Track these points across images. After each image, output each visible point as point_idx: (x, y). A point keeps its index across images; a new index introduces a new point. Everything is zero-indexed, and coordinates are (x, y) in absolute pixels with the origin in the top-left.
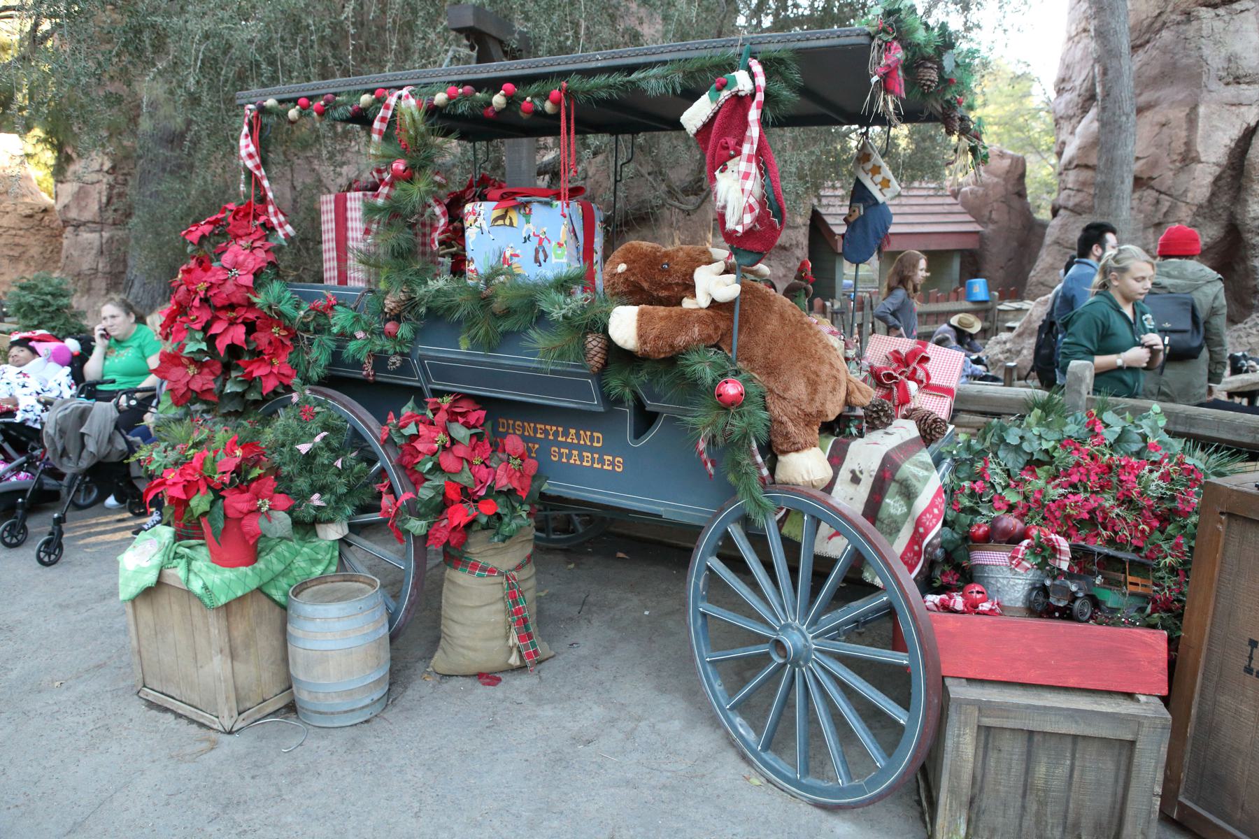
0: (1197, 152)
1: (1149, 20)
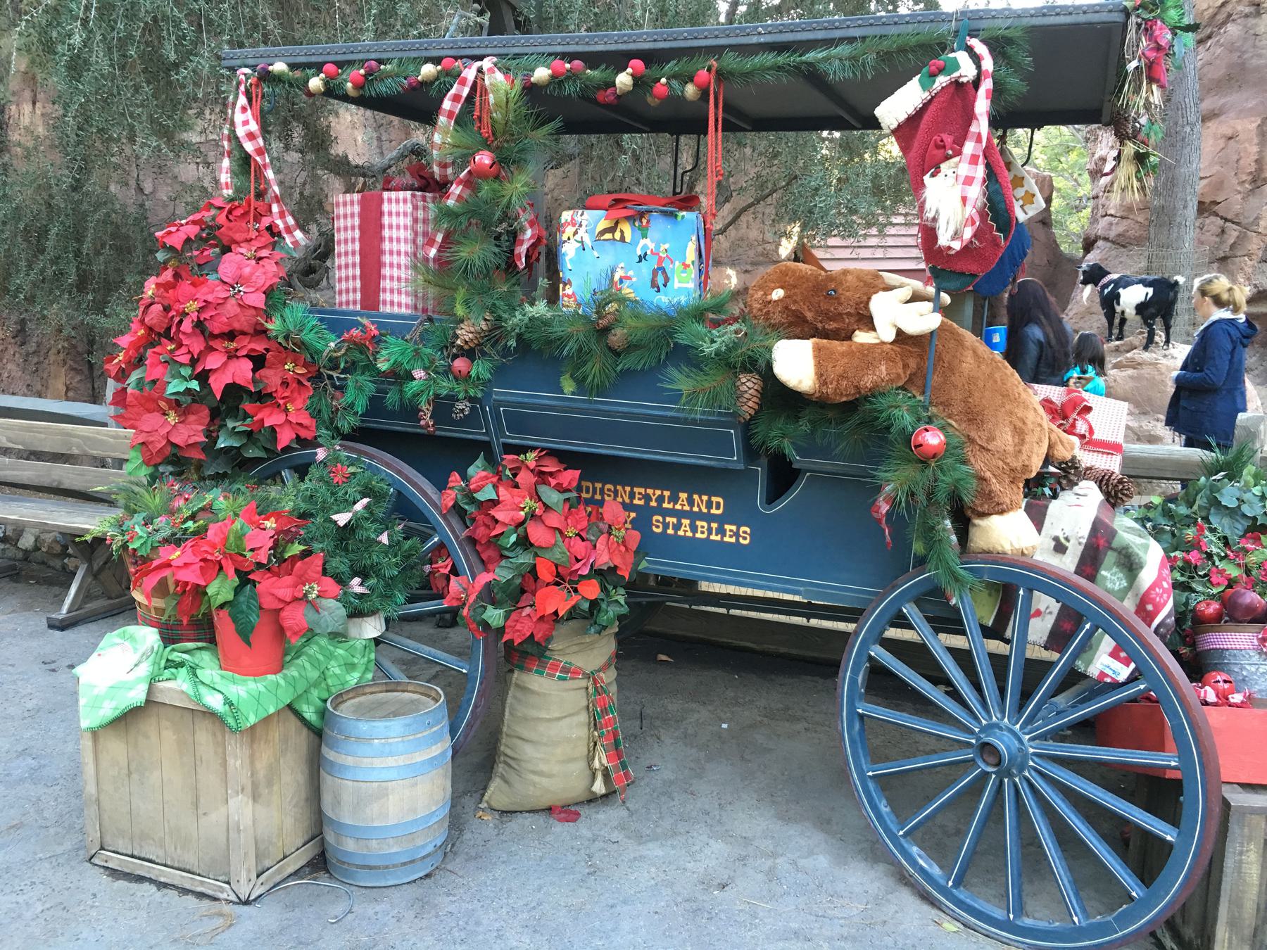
1: (1211, 10)
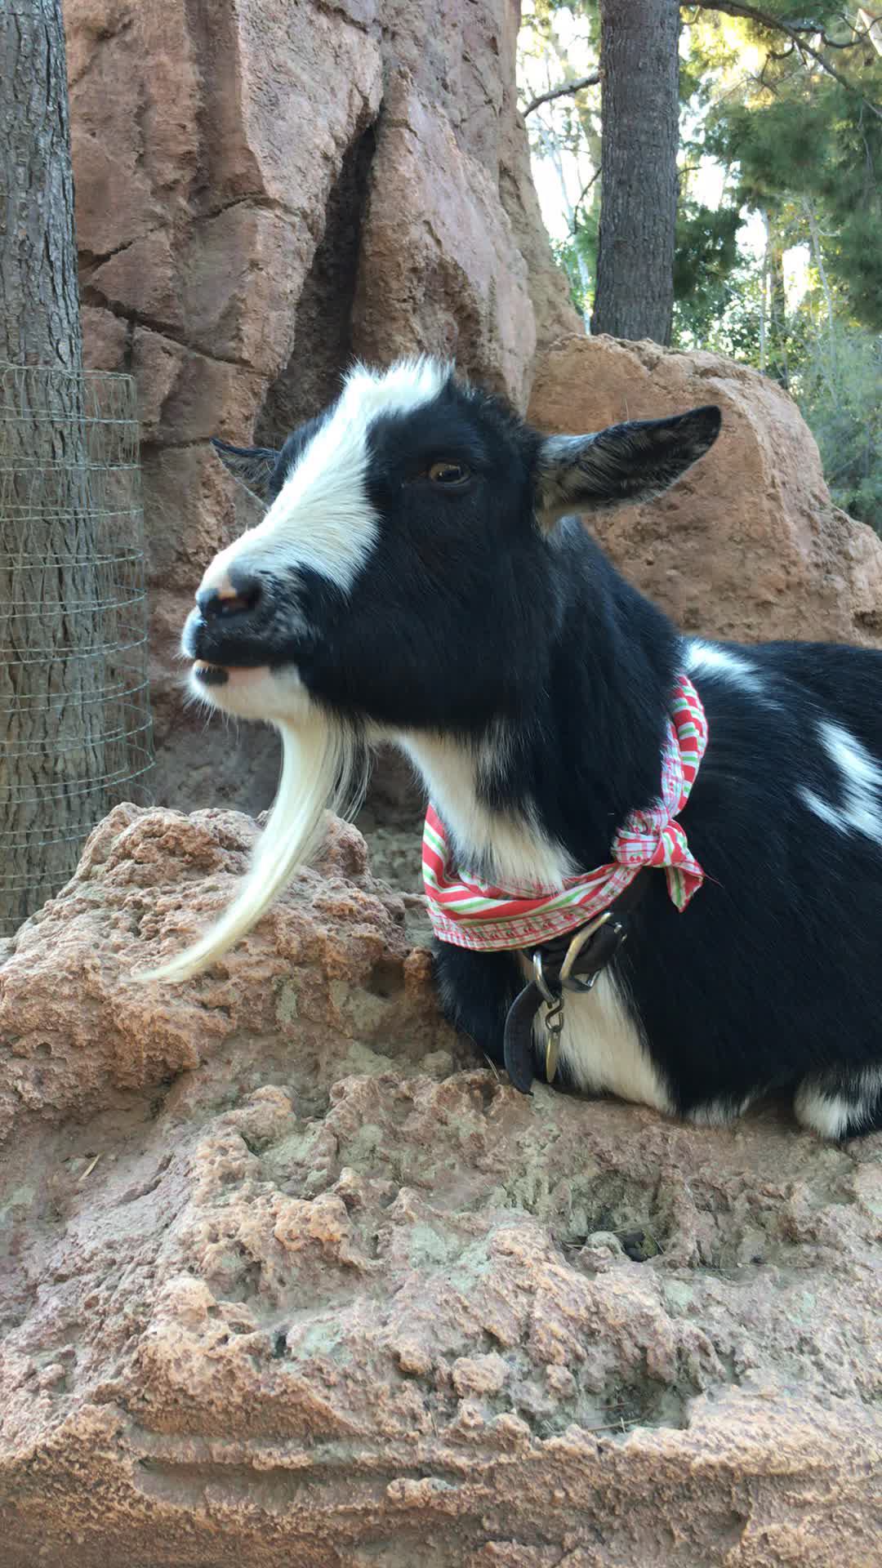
0: (250, 155)
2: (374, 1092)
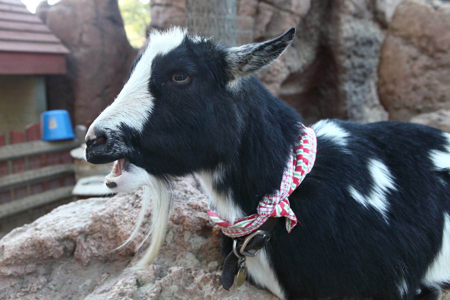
2: (181, 274)
